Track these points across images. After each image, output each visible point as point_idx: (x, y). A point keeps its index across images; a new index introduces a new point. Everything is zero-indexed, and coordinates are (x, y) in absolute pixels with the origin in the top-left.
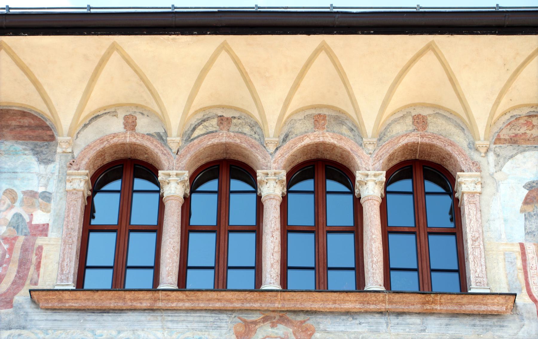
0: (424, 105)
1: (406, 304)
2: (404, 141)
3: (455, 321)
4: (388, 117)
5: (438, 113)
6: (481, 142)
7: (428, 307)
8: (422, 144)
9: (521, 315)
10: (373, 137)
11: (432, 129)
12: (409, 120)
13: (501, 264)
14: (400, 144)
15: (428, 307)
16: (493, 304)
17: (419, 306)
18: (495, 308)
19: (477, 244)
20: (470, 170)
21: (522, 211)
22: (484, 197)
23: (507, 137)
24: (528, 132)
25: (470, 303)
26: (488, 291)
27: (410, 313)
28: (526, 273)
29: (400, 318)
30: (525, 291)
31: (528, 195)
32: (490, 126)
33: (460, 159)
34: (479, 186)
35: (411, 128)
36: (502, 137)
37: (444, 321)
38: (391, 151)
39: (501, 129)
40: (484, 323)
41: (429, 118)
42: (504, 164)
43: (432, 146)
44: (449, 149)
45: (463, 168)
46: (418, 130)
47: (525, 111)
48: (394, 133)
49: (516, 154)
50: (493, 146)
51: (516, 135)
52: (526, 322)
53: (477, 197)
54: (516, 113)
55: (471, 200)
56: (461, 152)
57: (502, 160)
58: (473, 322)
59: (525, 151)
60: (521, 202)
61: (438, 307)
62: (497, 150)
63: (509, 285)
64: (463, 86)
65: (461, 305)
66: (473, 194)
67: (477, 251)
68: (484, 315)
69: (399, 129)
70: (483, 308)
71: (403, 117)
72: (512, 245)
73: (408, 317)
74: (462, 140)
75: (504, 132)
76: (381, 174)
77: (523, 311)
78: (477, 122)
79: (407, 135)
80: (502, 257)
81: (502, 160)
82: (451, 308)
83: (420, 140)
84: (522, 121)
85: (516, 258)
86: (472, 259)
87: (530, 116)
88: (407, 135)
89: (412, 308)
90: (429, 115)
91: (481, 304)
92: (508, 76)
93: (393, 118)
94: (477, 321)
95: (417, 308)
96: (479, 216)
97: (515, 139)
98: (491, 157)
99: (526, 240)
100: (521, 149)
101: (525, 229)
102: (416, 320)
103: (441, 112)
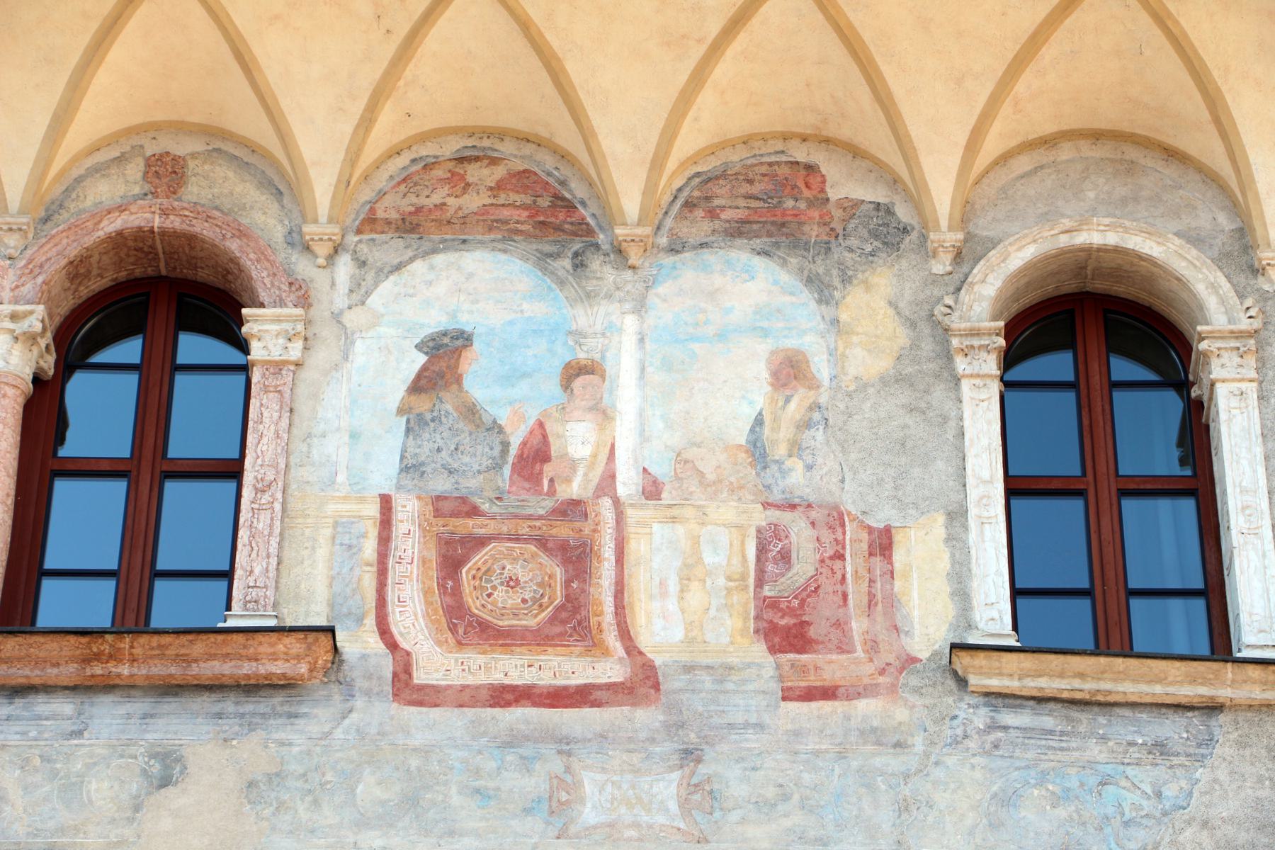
0: (180, 128)
1: (39, 662)
2: (112, 225)
3: (171, 704)
4: (75, 159)
5: (218, 150)
6: (320, 229)
7: (98, 670)
8: (164, 233)
9: (350, 685)
10: (22, 212)
11: (194, 191)
12: (135, 169)
13: (322, 552)
14: (101, 233)
15: (98, 670)
16: (274, 658)
17: (73, 668)
18: (278, 668)
19: (266, 498)
20: (281, 303)
21: (400, 411)
22: (306, 375)
23: (394, 215)
24: (451, 201)
25: (211, 657)
26: (272, 623)
27: (47, 689)
28: (382, 572)
29: (19, 702)
30: (370, 621)
31: (424, 368)
32: (344, 183)
33: (259, 275)
34: (298, 345)
35: (137, 190)
36: (380, 214)
37: (140, 705)
38: (73, 252)
39: (382, 194)
40: (249, 708)
41: (191, 164)
42: (376, 285)
43: (191, 239)
44: (233, 246)
45: (263, 296)
46: (155, 194)
47: (451, 146)
48: (88, 203)
49: (412, 260)
50: (352, 239)
51: (419, 210)
52: (359, 703)
53: (287, 376)
54: (428, 150)
55: (271, 382)
56: (263, 255)
57: (370, 277)
58: (217, 708)
59: (434, 251)
60: (405, 387)
61: (125, 670)
62: (364, 248)
63: (332, 605)
64: (272, 73)
65: (188, 660)
66: (277, 366)
67: (265, 517)
68: (251, 688)
69: (103, 191)
70: (247, 668)
71: (121, 159)
72: (362, 500)
73: (41, 698)
74: (272, 222)
75: (388, 201)
76: (31, 313)
77: (356, 674)
78: (312, 173)
79: (121, 209)
80: (328, 532)
81: (370, 277)
82: (159, 669)
83: (157, 222)
84: (439, 173)
85: (364, 535)
86: (246, 540)
87: (461, 160)
88: (121, 209)
89: (52, 674)
90: (194, 155)
91: (240, 658)
92: (389, 50)
93: (89, 162)
94: (229, 705)
95: (68, 672)
96: (284, 423)
97: (415, 219)
98: (344, 268)
99: (399, 487)
100: (426, 245)
101: (402, 458)
102: (64, 706)
103: (229, 147)
